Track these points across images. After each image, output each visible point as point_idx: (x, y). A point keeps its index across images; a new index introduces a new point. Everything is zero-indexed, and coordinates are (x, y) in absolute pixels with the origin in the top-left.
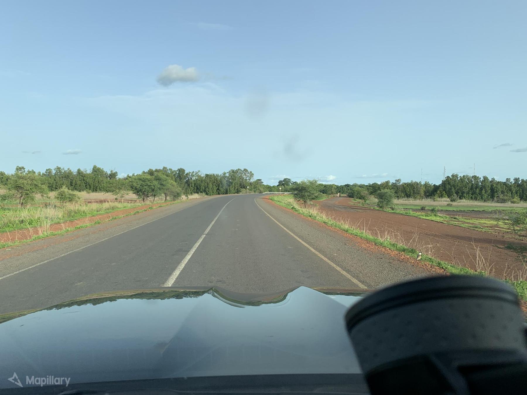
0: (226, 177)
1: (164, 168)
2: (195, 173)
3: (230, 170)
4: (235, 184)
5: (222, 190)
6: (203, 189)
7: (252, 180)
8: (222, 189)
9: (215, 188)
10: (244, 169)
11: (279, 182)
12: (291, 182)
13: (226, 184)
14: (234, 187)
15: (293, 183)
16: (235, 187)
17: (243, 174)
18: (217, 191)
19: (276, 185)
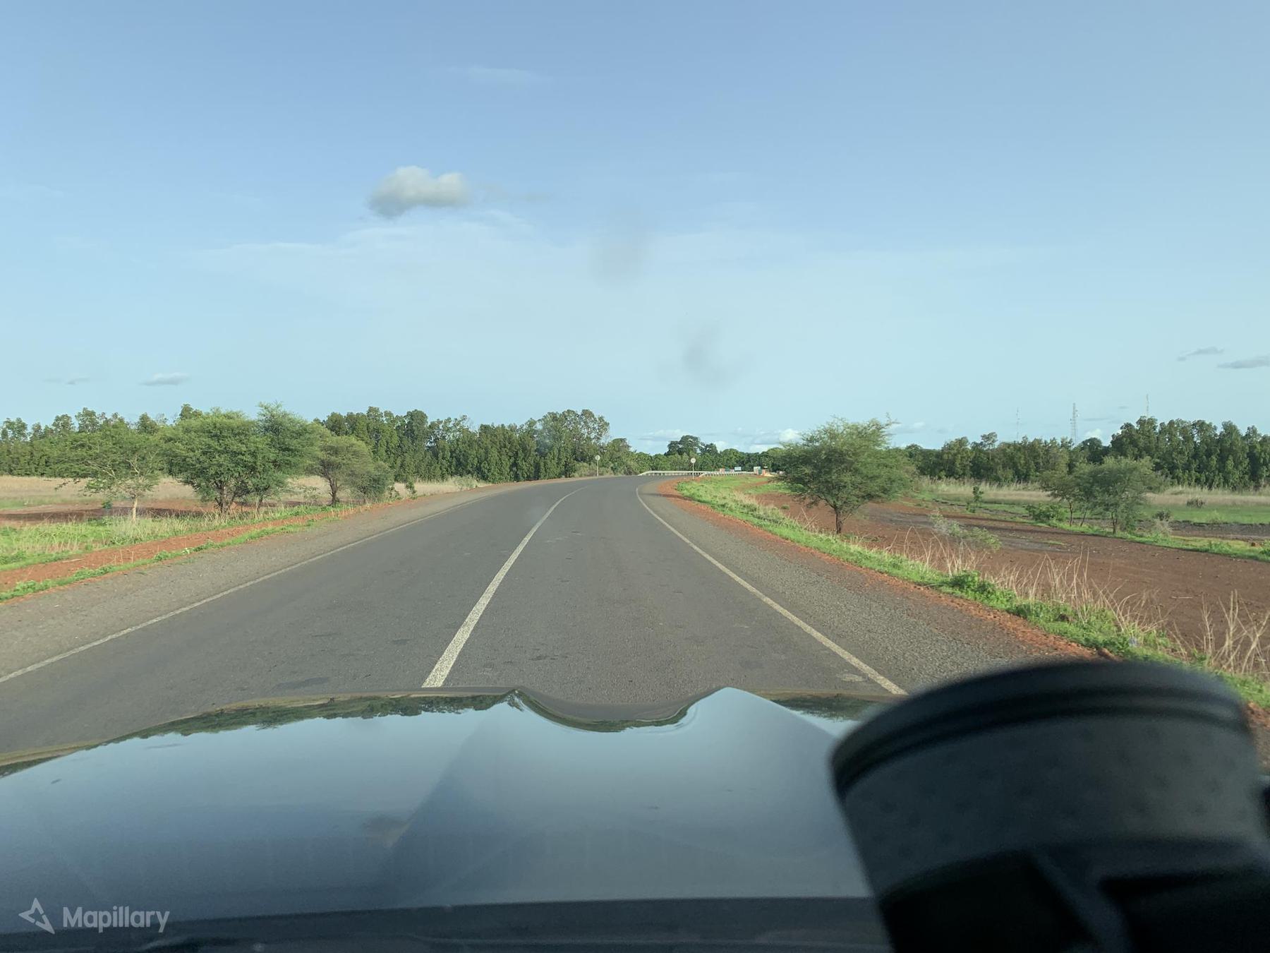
0: (536, 432)
1: (371, 409)
2: (452, 422)
3: (546, 414)
4: (559, 451)
6: (473, 464)
7: (605, 441)
8: (524, 463)
9: (507, 463)
10: (583, 411)
11: (670, 446)
12: (700, 445)
13: (535, 451)
14: (556, 459)
15: (703, 447)
16: (559, 459)
17: (580, 424)
18: (511, 470)
19: (663, 454)
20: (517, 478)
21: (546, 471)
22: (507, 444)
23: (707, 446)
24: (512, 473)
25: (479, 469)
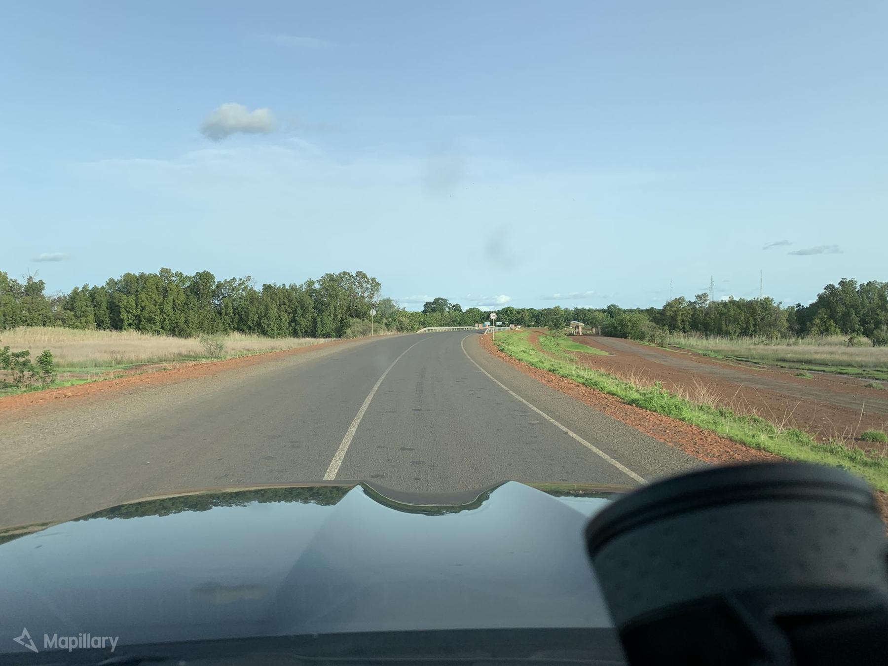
2: (237, 282)
5: (303, 323)
6: (253, 320)
9: (286, 318)
13: (313, 308)
18: (290, 325)
20: (295, 334)
21: (322, 326)
22: (286, 301)
24: (291, 328)
25: (259, 324)
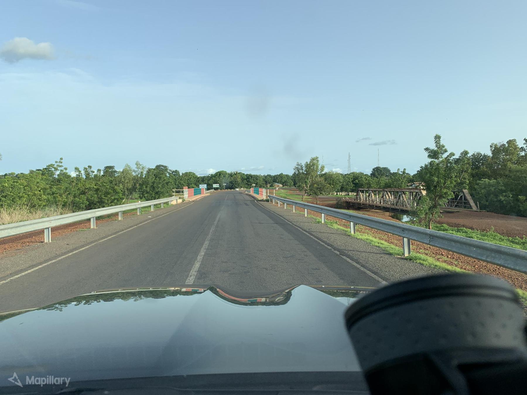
12: (169, 171)
15: (171, 172)
23: (173, 172)
